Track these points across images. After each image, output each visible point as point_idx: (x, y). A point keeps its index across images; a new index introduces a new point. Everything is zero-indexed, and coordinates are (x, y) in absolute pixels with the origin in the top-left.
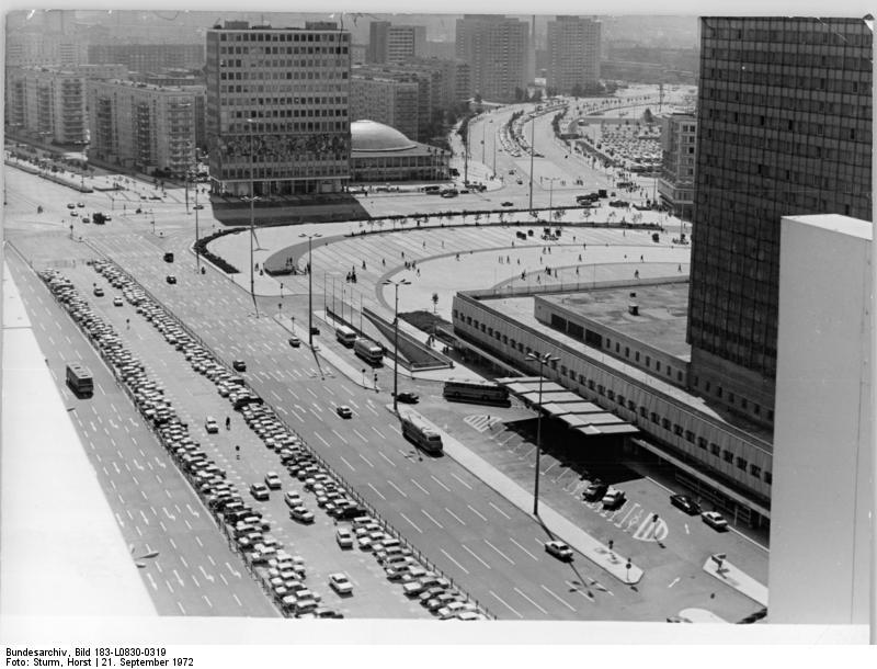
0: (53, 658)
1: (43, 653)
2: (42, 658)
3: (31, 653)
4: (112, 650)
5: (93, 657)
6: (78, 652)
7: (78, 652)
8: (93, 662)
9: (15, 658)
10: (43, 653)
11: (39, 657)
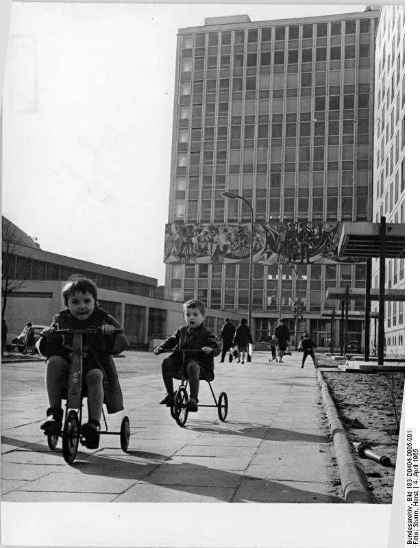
0: (413, 515)
1: (410, 521)
2: (413, 521)
3: (410, 529)
4: (408, 478)
5: (412, 490)
6: (409, 500)
7: (409, 500)
8: (416, 490)
9: (413, 538)
10: (410, 521)
11: (412, 524)
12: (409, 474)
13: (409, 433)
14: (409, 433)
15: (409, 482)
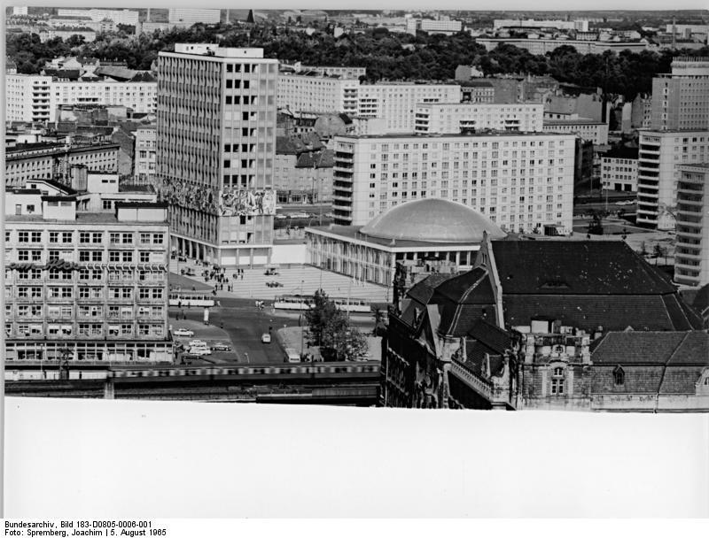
1: (35, 525)
3: (25, 525)
4: (91, 523)
7: (63, 524)
10: (35, 525)
12: (95, 524)
13: (148, 525)
14: (148, 525)
15: (85, 524)
